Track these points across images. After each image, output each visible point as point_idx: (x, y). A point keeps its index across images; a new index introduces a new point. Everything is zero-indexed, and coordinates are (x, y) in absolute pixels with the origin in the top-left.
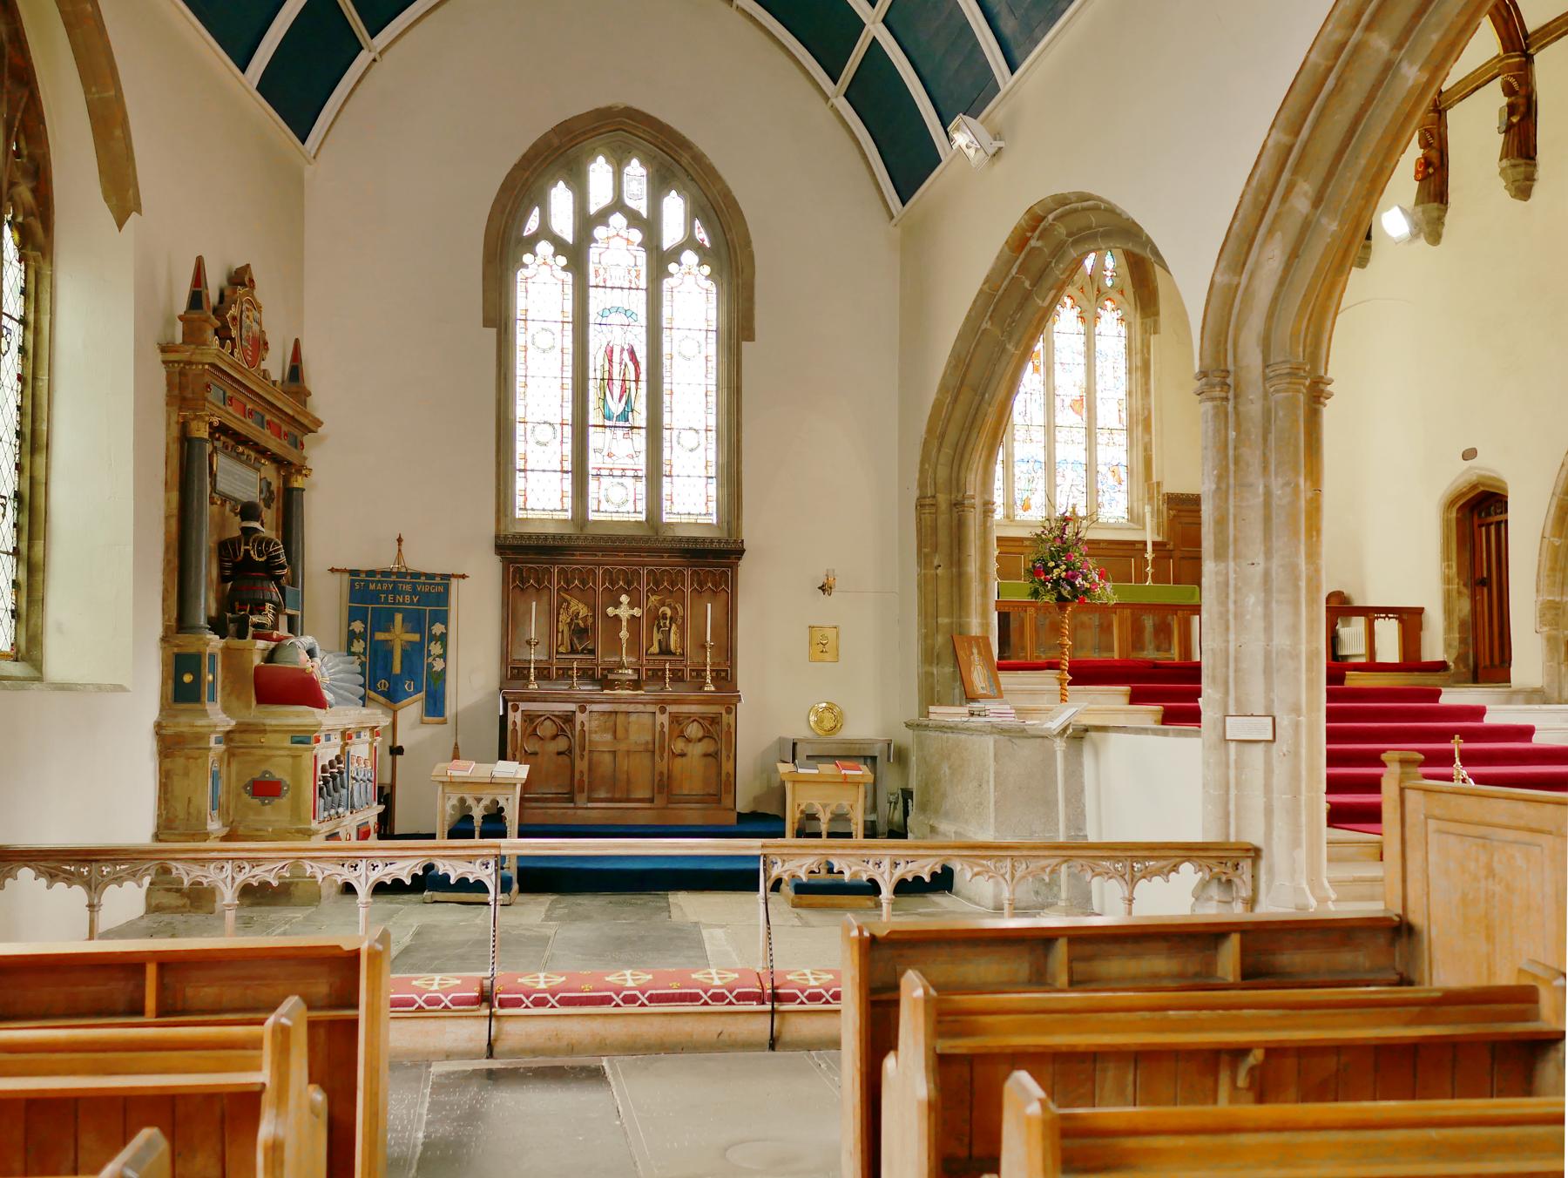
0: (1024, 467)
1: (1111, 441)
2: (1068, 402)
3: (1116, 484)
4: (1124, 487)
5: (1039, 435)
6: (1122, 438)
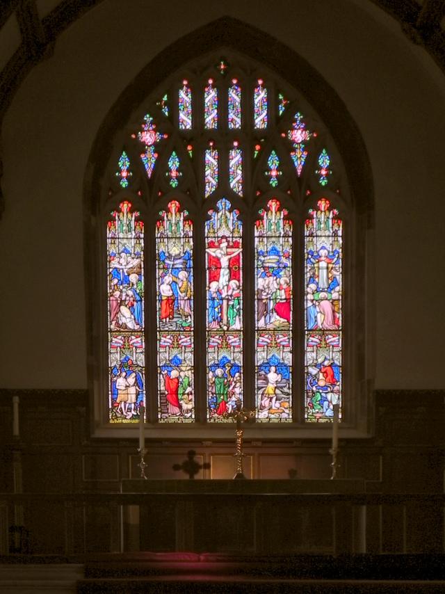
0: (219, 372)
1: (323, 343)
2: (271, 305)
3: (328, 384)
4: (338, 387)
5: (236, 341)
6: (336, 340)
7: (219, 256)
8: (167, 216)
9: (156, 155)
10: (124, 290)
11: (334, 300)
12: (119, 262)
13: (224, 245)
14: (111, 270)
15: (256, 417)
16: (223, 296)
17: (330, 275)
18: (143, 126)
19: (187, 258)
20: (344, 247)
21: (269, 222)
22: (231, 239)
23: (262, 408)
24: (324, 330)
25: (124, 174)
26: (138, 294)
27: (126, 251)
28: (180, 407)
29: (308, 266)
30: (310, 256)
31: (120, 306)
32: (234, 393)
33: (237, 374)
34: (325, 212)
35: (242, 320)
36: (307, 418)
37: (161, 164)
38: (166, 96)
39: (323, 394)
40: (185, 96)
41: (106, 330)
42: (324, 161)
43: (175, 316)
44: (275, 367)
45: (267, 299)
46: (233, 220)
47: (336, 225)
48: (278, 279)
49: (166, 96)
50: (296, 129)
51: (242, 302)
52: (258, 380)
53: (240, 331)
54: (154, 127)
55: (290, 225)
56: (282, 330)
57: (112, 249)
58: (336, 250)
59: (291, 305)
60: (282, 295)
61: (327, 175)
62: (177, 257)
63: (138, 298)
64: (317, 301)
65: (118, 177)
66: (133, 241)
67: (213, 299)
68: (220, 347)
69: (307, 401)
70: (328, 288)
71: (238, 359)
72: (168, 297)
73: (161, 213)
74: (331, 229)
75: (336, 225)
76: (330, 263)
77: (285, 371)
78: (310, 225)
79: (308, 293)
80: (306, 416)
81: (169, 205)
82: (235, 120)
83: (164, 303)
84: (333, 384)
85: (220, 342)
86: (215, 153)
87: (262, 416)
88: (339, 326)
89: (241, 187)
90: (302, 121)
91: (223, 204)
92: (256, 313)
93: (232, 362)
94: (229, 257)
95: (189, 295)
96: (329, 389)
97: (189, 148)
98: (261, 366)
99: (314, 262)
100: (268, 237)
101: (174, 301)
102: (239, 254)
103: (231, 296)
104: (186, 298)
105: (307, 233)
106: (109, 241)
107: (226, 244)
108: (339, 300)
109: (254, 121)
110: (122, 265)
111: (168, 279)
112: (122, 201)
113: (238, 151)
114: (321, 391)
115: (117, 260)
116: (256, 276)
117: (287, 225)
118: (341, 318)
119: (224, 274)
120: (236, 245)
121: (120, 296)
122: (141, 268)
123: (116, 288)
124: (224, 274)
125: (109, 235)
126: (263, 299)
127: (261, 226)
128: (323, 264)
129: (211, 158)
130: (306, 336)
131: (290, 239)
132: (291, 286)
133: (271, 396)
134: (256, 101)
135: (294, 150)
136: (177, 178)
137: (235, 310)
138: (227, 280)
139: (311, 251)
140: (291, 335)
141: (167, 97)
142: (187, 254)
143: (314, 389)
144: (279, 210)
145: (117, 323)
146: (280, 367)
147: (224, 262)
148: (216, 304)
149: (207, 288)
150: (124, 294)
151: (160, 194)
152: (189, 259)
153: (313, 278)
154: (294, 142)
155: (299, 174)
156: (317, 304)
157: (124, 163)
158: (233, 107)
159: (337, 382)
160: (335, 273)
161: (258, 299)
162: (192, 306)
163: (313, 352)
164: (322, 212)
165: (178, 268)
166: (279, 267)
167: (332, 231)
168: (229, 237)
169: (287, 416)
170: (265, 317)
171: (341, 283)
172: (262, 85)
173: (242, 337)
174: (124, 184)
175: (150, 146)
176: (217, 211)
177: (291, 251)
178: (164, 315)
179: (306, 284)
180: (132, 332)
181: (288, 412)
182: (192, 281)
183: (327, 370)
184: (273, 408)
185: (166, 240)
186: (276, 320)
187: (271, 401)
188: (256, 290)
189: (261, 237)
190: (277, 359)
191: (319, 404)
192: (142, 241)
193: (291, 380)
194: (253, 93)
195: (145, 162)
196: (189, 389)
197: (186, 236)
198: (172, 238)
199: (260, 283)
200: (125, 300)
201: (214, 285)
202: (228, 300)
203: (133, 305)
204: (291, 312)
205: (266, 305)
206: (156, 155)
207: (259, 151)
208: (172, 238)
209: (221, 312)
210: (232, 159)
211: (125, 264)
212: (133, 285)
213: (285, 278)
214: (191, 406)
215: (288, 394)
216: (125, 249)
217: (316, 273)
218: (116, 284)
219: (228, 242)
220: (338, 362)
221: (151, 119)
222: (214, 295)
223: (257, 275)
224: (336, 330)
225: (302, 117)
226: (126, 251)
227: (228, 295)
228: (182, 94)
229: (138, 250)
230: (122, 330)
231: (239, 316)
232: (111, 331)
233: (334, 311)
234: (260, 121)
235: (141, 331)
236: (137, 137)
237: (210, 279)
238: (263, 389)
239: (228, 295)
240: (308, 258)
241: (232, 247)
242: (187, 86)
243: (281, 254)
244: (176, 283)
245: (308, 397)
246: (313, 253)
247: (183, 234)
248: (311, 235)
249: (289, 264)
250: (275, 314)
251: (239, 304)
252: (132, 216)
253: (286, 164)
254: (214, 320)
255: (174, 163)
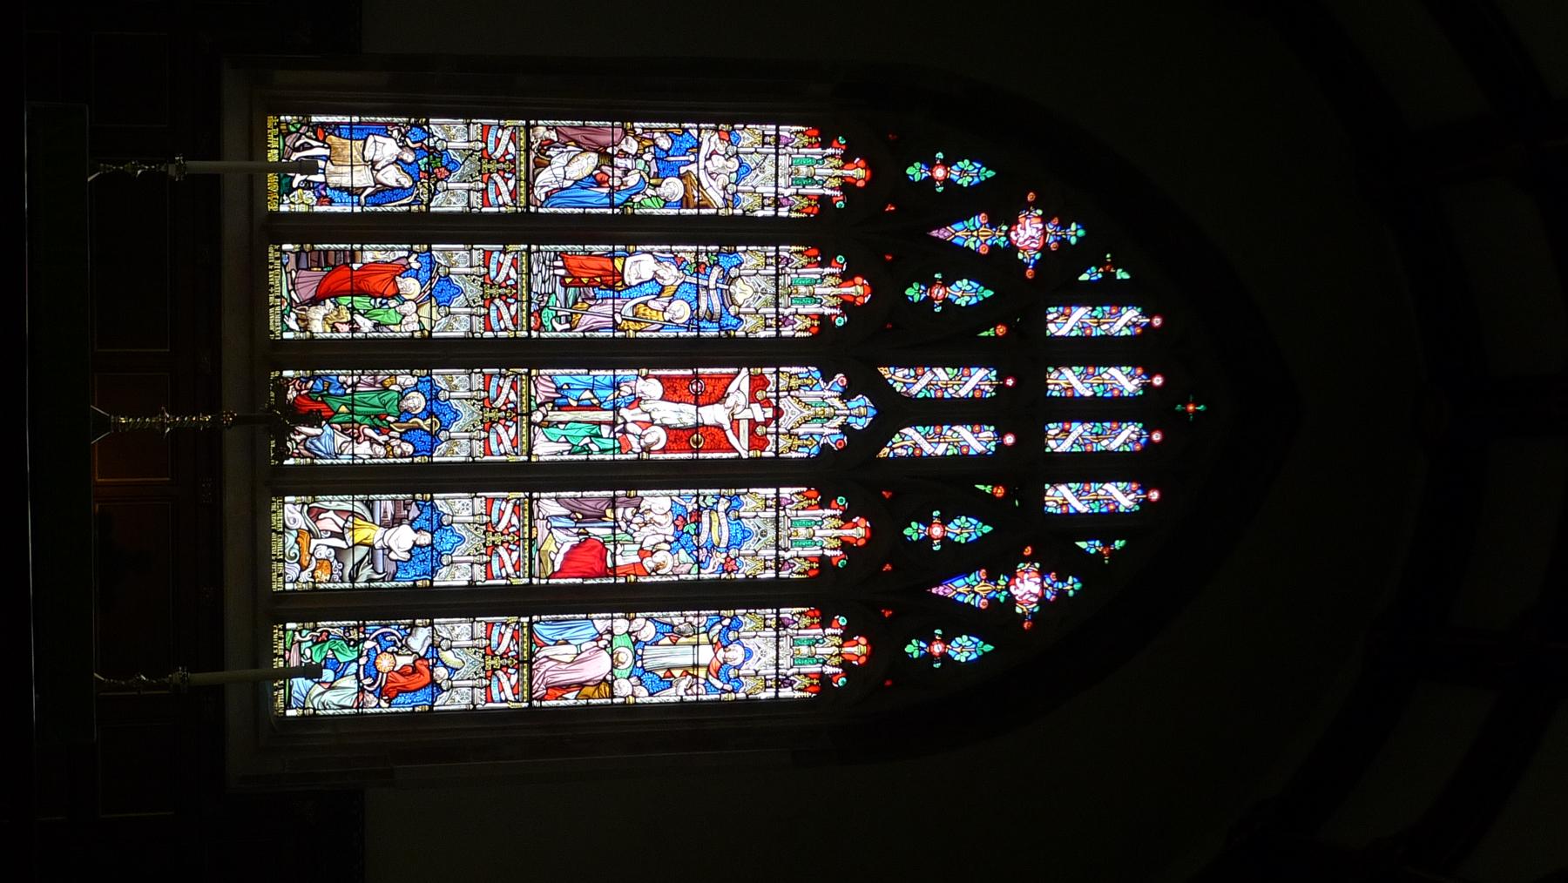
0: (416, 401)
1: (496, 662)
2: (599, 531)
4: (372, 705)
5: (503, 445)
6: (505, 693)
7: (730, 402)
8: (832, 275)
9: (984, 251)
10: (641, 164)
11: (611, 686)
12: (714, 153)
13: (759, 413)
14: (694, 133)
15: (287, 499)
16: (623, 412)
17: (677, 673)
18: (1056, 221)
19: (724, 323)
20: (750, 704)
21: (816, 523)
22: (772, 429)
23: (315, 514)
24: (530, 663)
25: (939, 173)
26: (630, 199)
27: (743, 170)
28: (316, 301)
29: (704, 618)
30: (726, 622)
31: (596, 151)
32: (355, 439)
33: (409, 448)
34: (840, 654)
35: (559, 458)
36: (285, 630)
37: (961, 263)
38: (1126, 276)
39: (354, 667)
40: (1125, 321)
41: (532, 113)
42: (965, 649)
43: (571, 291)
44: (431, 545)
45: (615, 520)
46: (821, 435)
47: (806, 682)
48: (667, 547)
49: (1126, 276)
50: (1043, 579)
51: (608, 457)
52: (394, 500)
53: (529, 454)
54: (1053, 246)
55: (805, 572)
56: (531, 559)
57: (749, 136)
58: (742, 684)
59: (598, 581)
60: (627, 557)
61: (929, 657)
62: (727, 299)
63: (618, 198)
64: (611, 642)
65: (935, 160)
66: (769, 190)
67: (615, 386)
68: (486, 404)
69: (335, 627)
70: (645, 671)
71: (456, 449)
72: (622, 274)
73: (840, 259)
74: (795, 670)
75: (806, 682)
76: (708, 670)
77: (420, 569)
78: (805, 621)
79: (631, 620)
80: (290, 626)
81: (859, 280)
82: (1065, 439)
83: (607, 264)
84: (381, 693)
85: (499, 403)
86: (989, 392)
87: (292, 512)
88: (541, 699)
89: (902, 452)
90: (1061, 594)
91: (861, 412)
92: (579, 494)
93: (443, 435)
94: (727, 426)
95: (625, 325)
96: (369, 681)
97: (1001, 330)
98: (433, 508)
99: (711, 634)
100: (777, 519)
101: (612, 288)
102: (734, 450)
103: (624, 431)
104: (618, 318)
105: (786, 613)
106: (770, 129)
107: (760, 418)
108: (613, 696)
109: (1065, 481)
110: (706, 160)
111: (670, 275)
112: (869, 166)
113: (992, 446)
114: (363, 661)
115: (721, 148)
116: (676, 492)
117: (806, 565)
118: (562, 703)
119: (682, 414)
120: (757, 441)
121: (626, 155)
122: (698, 207)
123: (646, 143)
124: (682, 414)
125: (785, 131)
126: (614, 508)
127: (805, 504)
128: (706, 655)
129: (977, 381)
130: (515, 619)
131: (770, 574)
132: (648, 579)
133: (348, 535)
134: (1110, 487)
135: (992, 577)
136: (929, 300)
137: (587, 440)
138: (666, 422)
139: (741, 623)
140: (516, 582)
141: (1122, 280)
142: (735, 321)
143: (369, 644)
144: (846, 545)
145: (551, 144)
146: (432, 556)
147: (713, 414)
148: (600, 393)
149: (644, 371)
150: (629, 163)
151: (889, 258)
152: (721, 328)
153: (675, 634)
154: (1012, 575)
155: (934, 591)
156: (602, 644)
157: (968, 173)
158: (1097, 434)
159: (389, 701)
160: (684, 683)
161: (614, 499)
162: (596, 334)
163: (472, 639)
164: (840, 646)
165: (697, 298)
166: (698, 548)
167: (789, 673)
168: (778, 427)
169: (292, 577)
170: (568, 517)
171: (655, 700)
172: (1147, 500)
173: (512, 459)
174: (916, 172)
175: (1007, 234)
176: (846, 396)
177: (740, 576)
178: (572, 262)
179: (655, 614)
180: (527, 180)
181: (301, 580)
182: (663, 334)
183: (423, 672)
184: (314, 542)
185: (772, 270)
186: (557, 544)
187: (334, 535)
188: (640, 493)
189: (778, 504)
190: (453, 549)
191: (325, 658)
192: (769, 212)
193: (393, 584)
194: (1129, 481)
195: (969, 223)
196: (366, 325)
197: (781, 321)
198: (777, 285)
199: (658, 502)
200: (613, 166)
201: (653, 389)
202: (613, 424)
203: (600, 184)
204: (579, 581)
205: (601, 517)
206: (984, 251)
207: (992, 495)
208: (777, 285)
209: (580, 408)
210: (973, 432)
211: (711, 169)
212: (655, 186)
213: (673, 565)
214: (318, 328)
215: (353, 579)
216: (749, 170)
217: (683, 640)
218: (656, 145)
219: (766, 423)
220: (444, 702)
221: (1073, 240)
222: (625, 390)
223: (679, 496)
224: (530, 693)
225: (1071, 593)
226: (743, 170)
227: (625, 423)
228: (1131, 314)
229: (747, 201)
230: (532, 155)
231: (570, 453)
232: (528, 127)
233: (581, 685)
234: (1063, 497)
235: (528, 204)
236: (1027, 206)
237: (669, 378)
238: (367, 515)
239: (625, 423)
240: (722, 618)
241: (752, 432)
242: (1150, 324)
243: (733, 553)
244: (659, 296)
245: (347, 629)
246: (737, 630)
247: (787, 312)
248: (781, 624)
249: (706, 575)
250: (575, 540)
251: (602, 451)
252: (832, 189)
253: (960, 559)
254: (558, 389)
255: (965, 292)
